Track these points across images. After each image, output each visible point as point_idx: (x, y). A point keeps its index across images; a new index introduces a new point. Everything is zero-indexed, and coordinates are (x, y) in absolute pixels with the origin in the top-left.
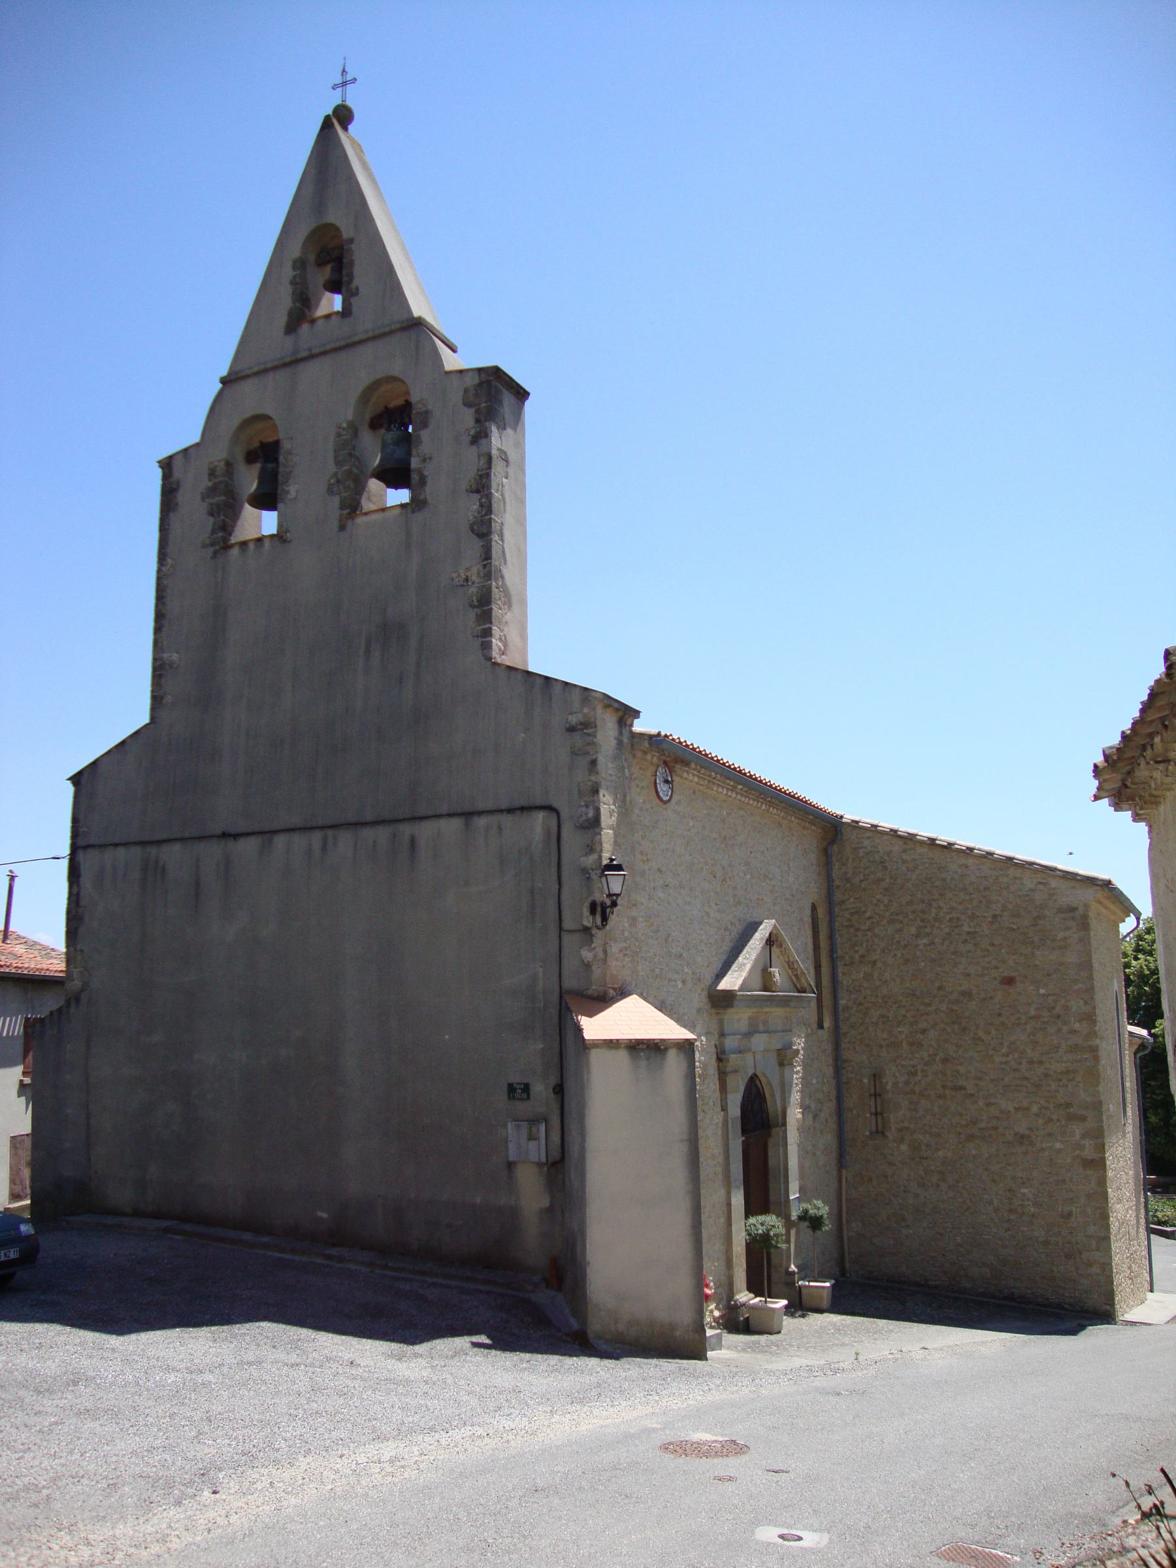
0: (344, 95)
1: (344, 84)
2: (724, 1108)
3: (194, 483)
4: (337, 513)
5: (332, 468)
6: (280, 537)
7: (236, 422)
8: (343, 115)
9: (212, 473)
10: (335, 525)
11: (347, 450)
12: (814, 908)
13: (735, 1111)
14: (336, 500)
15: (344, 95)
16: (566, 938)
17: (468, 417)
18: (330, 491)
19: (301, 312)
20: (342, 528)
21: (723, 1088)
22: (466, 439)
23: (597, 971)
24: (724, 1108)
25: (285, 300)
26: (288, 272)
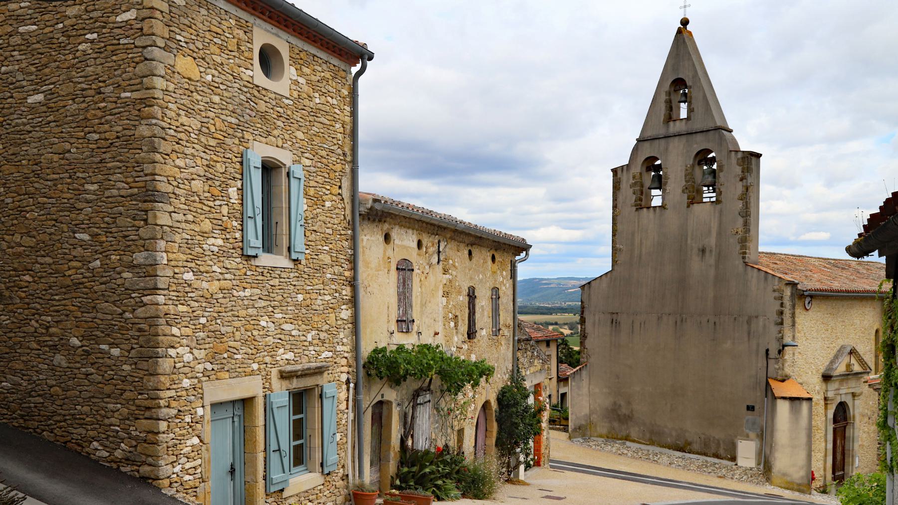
0: (685, 11)
1: (685, 7)
2: (826, 416)
3: (627, 180)
4: (686, 201)
5: (684, 183)
6: (663, 207)
7: (643, 159)
8: (685, 22)
9: (634, 177)
10: (686, 205)
11: (689, 176)
12: (877, 331)
13: (831, 415)
14: (686, 196)
15: (685, 11)
16: (770, 361)
17: (738, 170)
18: (683, 191)
19: (671, 116)
20: (688, 207)
21: (826, 408)
22: (738, 179)
23: (780, 372)
24: (826, 416)
25: (662, 107)
26: (663, 97)
